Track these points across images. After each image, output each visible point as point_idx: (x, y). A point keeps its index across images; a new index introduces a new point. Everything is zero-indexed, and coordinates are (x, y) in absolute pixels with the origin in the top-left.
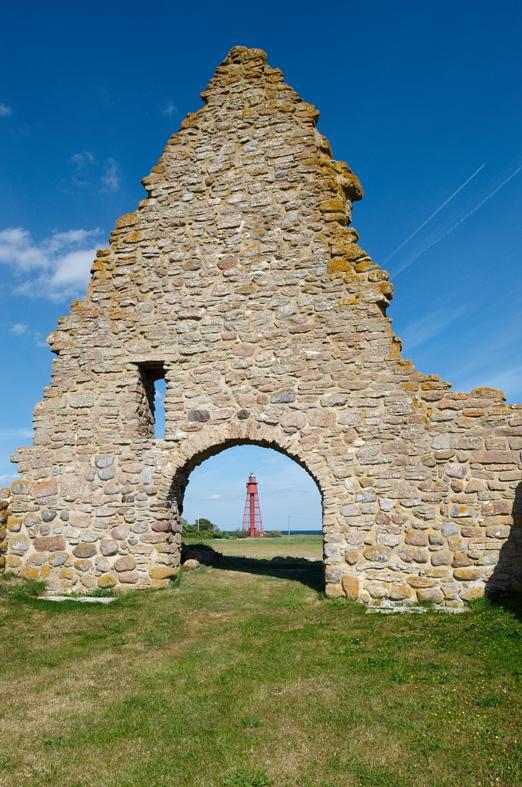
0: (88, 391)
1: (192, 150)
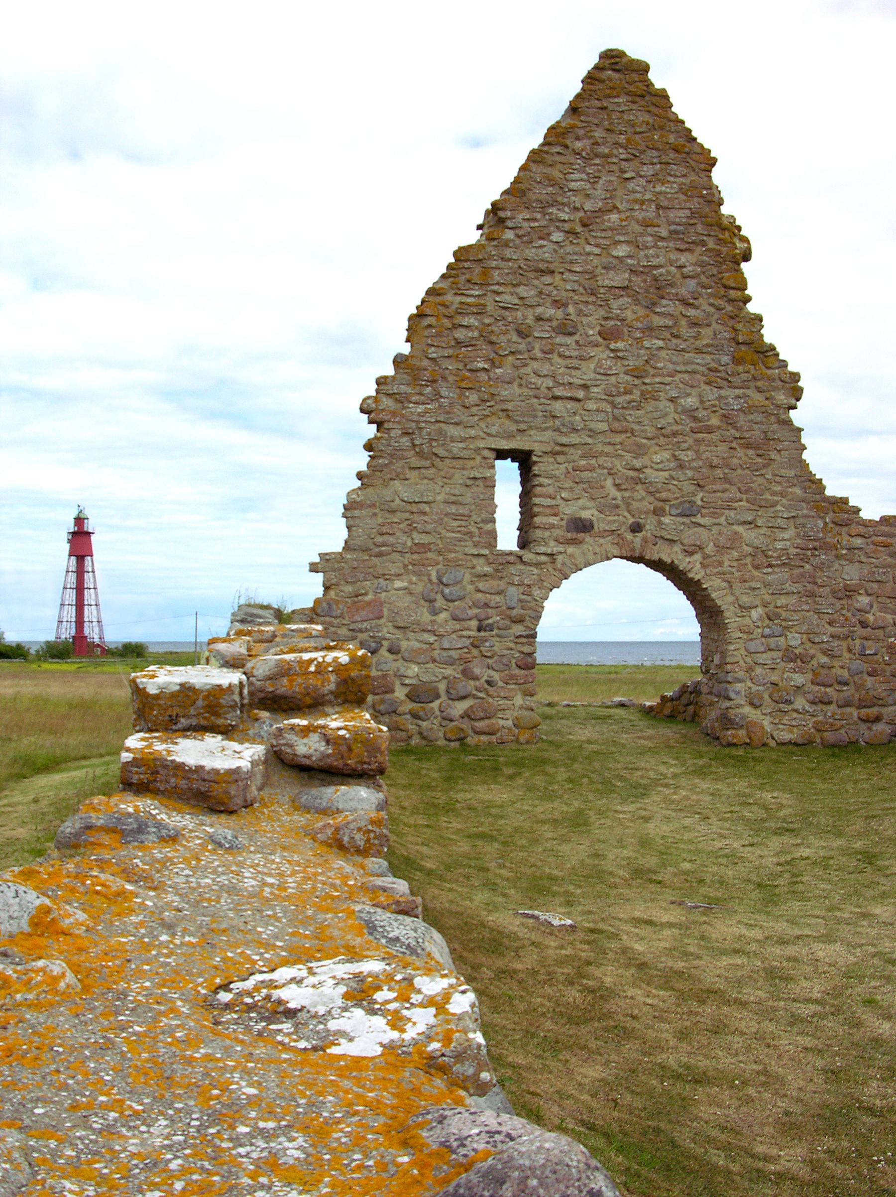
0: (425, 481)
1: (562, 176)
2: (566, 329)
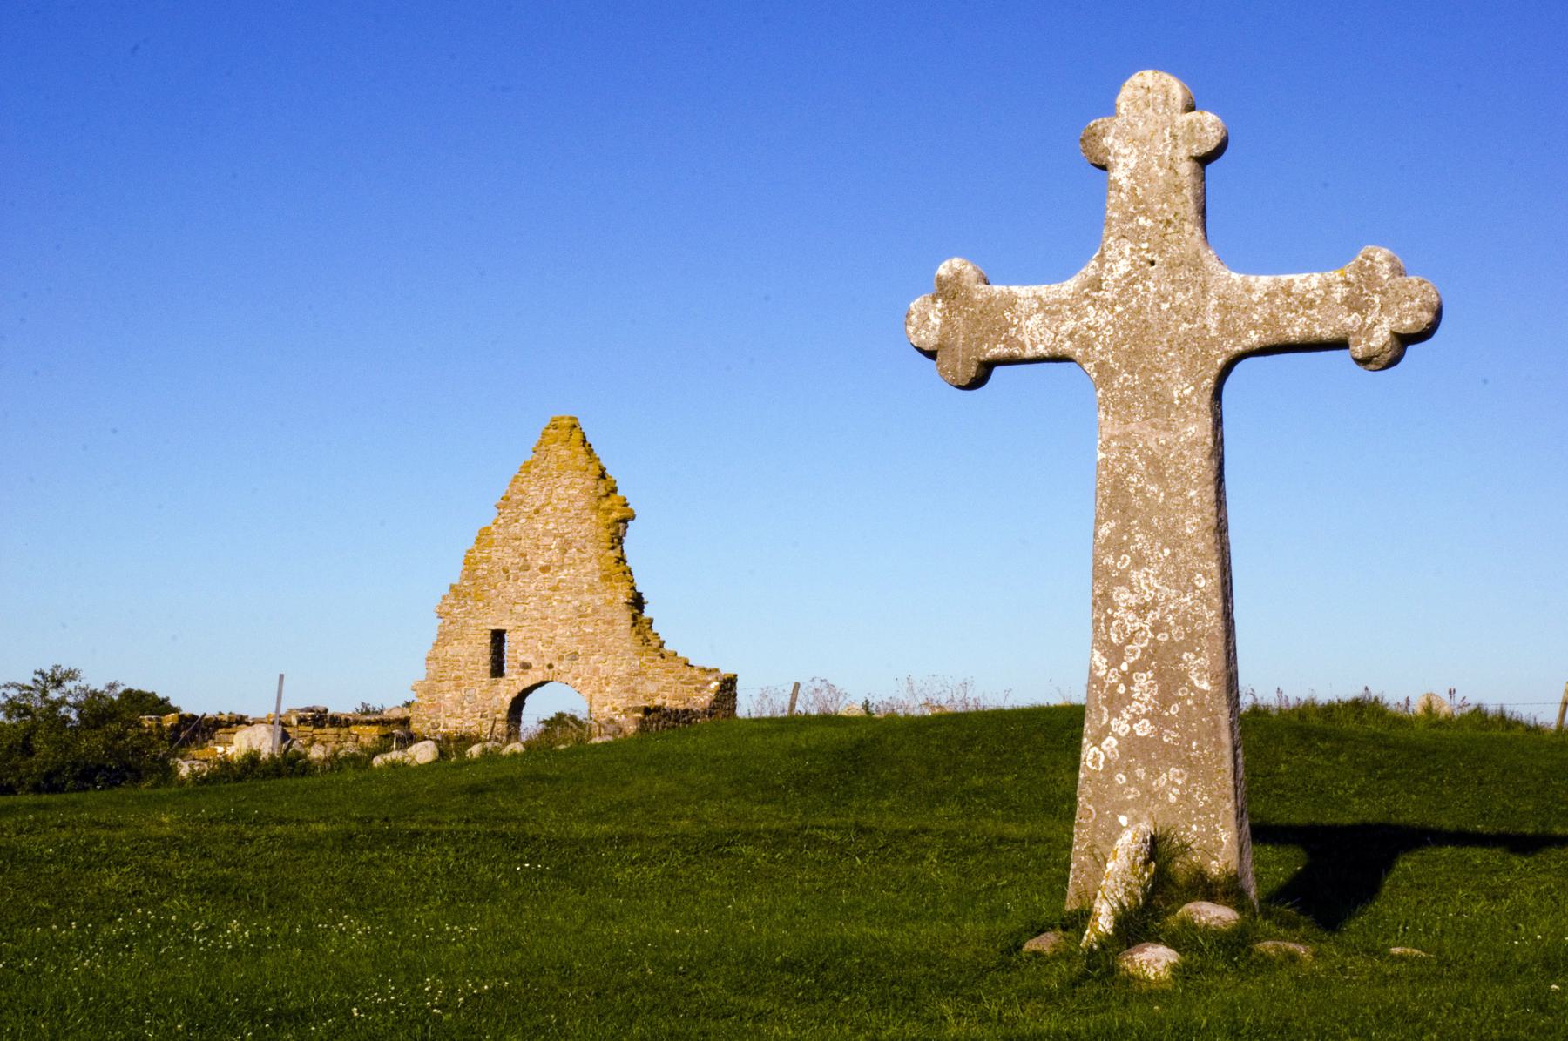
2: (526, 568)
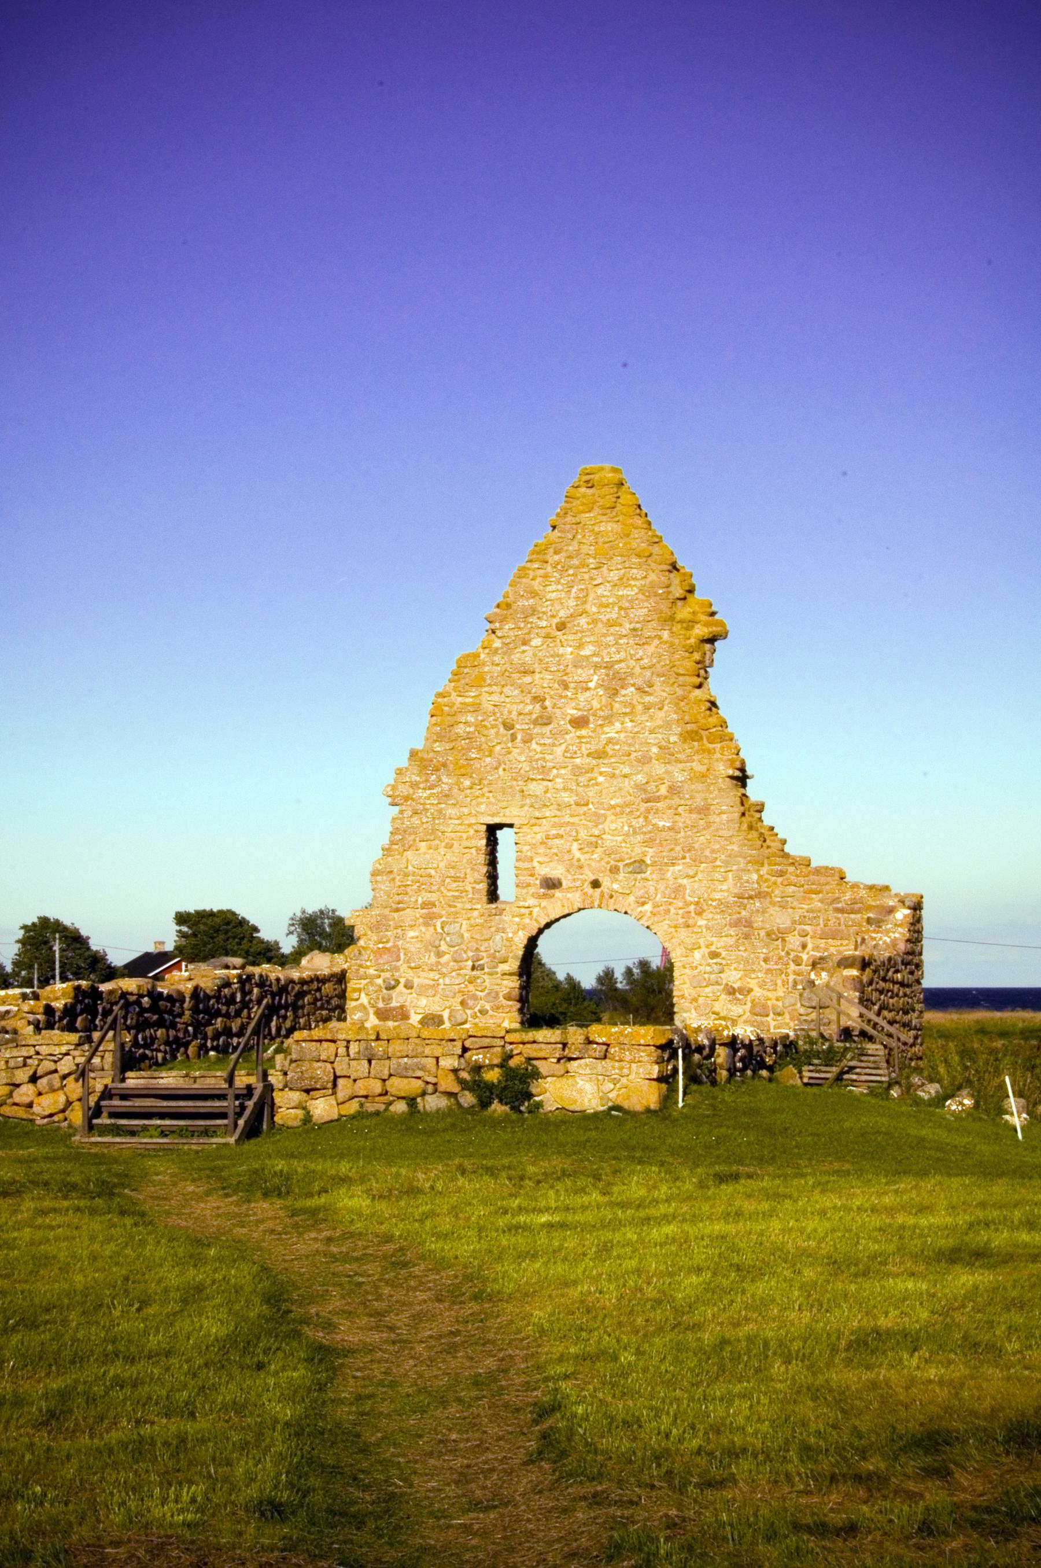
2: (545, 720)
